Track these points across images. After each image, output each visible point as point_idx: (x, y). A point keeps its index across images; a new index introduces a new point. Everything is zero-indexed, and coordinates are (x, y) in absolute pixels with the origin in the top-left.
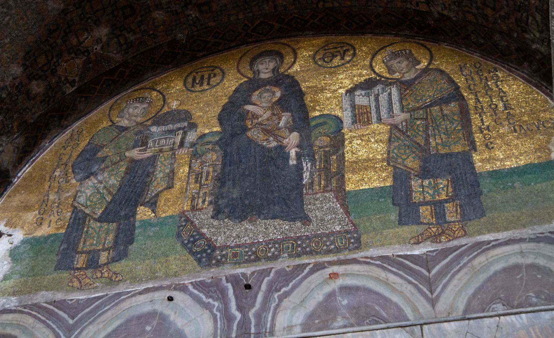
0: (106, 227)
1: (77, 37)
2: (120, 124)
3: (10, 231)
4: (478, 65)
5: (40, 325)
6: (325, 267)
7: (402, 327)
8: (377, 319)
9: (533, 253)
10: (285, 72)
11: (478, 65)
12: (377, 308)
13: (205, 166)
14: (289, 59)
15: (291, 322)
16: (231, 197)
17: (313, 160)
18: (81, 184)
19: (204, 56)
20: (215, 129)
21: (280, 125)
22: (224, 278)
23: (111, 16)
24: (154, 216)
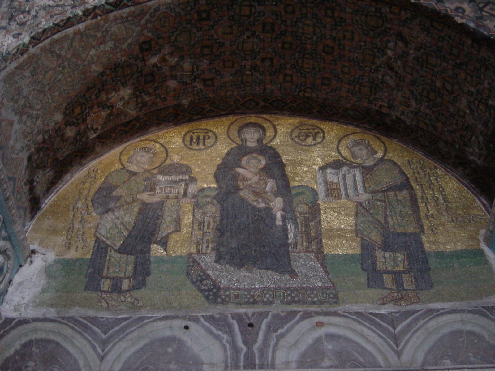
0: (125, 258)
1: (107, 95)
2: (130, 169)
3: (43, 251)
4: (422, 162)
5: (77, 336)
6: (312, 316)
10: (268, 143)
11: (422, 162)
12: (356, 354)
13: (207, 216)
14: (270, 133)
16: (230, 246)
17: (296, 224)
18: (101, 218)
19: (198, 119)
20: (212, 186)
22: (230, 316)
23: (136, 80)
24: (166, 254)
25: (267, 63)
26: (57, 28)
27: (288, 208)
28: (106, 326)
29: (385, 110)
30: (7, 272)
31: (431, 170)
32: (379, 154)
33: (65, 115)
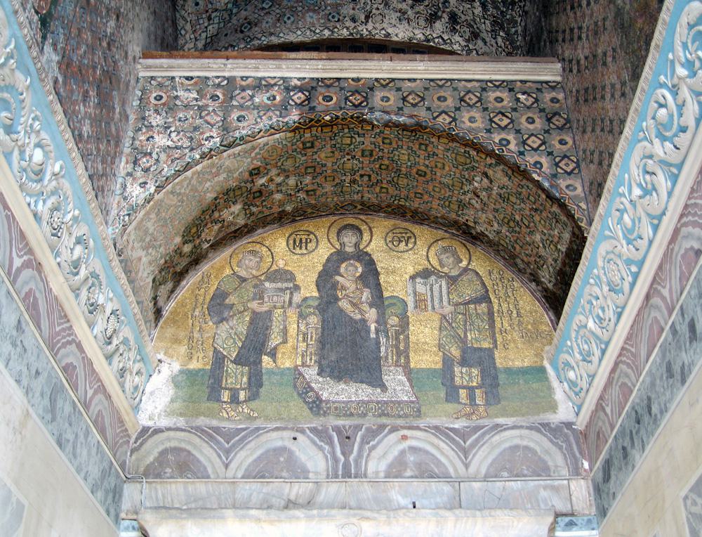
3: (169, 360)
4: (501, 273)
5: (205, 445)
6: (398, 430)
8: (432, 476)
12: (432, 466)
14: (366, 237)
17: (387, 337)
25: (366, 178)
26: (178, 173)
27: (382, 321)
28: (228, 436)
29: (472, 225)
32: (463, 263)
33: (183, 236)
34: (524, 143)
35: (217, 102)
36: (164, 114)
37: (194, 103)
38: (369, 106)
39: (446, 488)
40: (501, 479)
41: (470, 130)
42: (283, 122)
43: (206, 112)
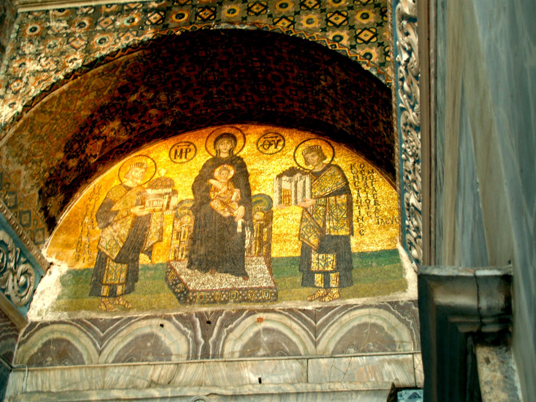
1: (99, 129)
3: (59, 263)
4: (362, 166)
5: (83, 335)
6: (255, 313)
7: (297, 359)
8: (283, 354)
9: (376, 316)
12: (284, 345)
14: (240, 143)
15: (233, 349)
17: (252, 231)
18: (102, 231)
21: (232, 199)
22: (194, 314)
26: (44, 93)
27: (248, 217)
28: (104, 325)
30: (30, 285)
31: (369, 173)
32: (327, 160)
33: (65, 152)
34: (357, 37)
35: (84, 28)
36: (37, 43)
37: (64, 31)
38: (217, 19)
39: (295, 365)
40: (347, 355)
41: (307, 31)
42: (138, 41)
43: (73, 38)
